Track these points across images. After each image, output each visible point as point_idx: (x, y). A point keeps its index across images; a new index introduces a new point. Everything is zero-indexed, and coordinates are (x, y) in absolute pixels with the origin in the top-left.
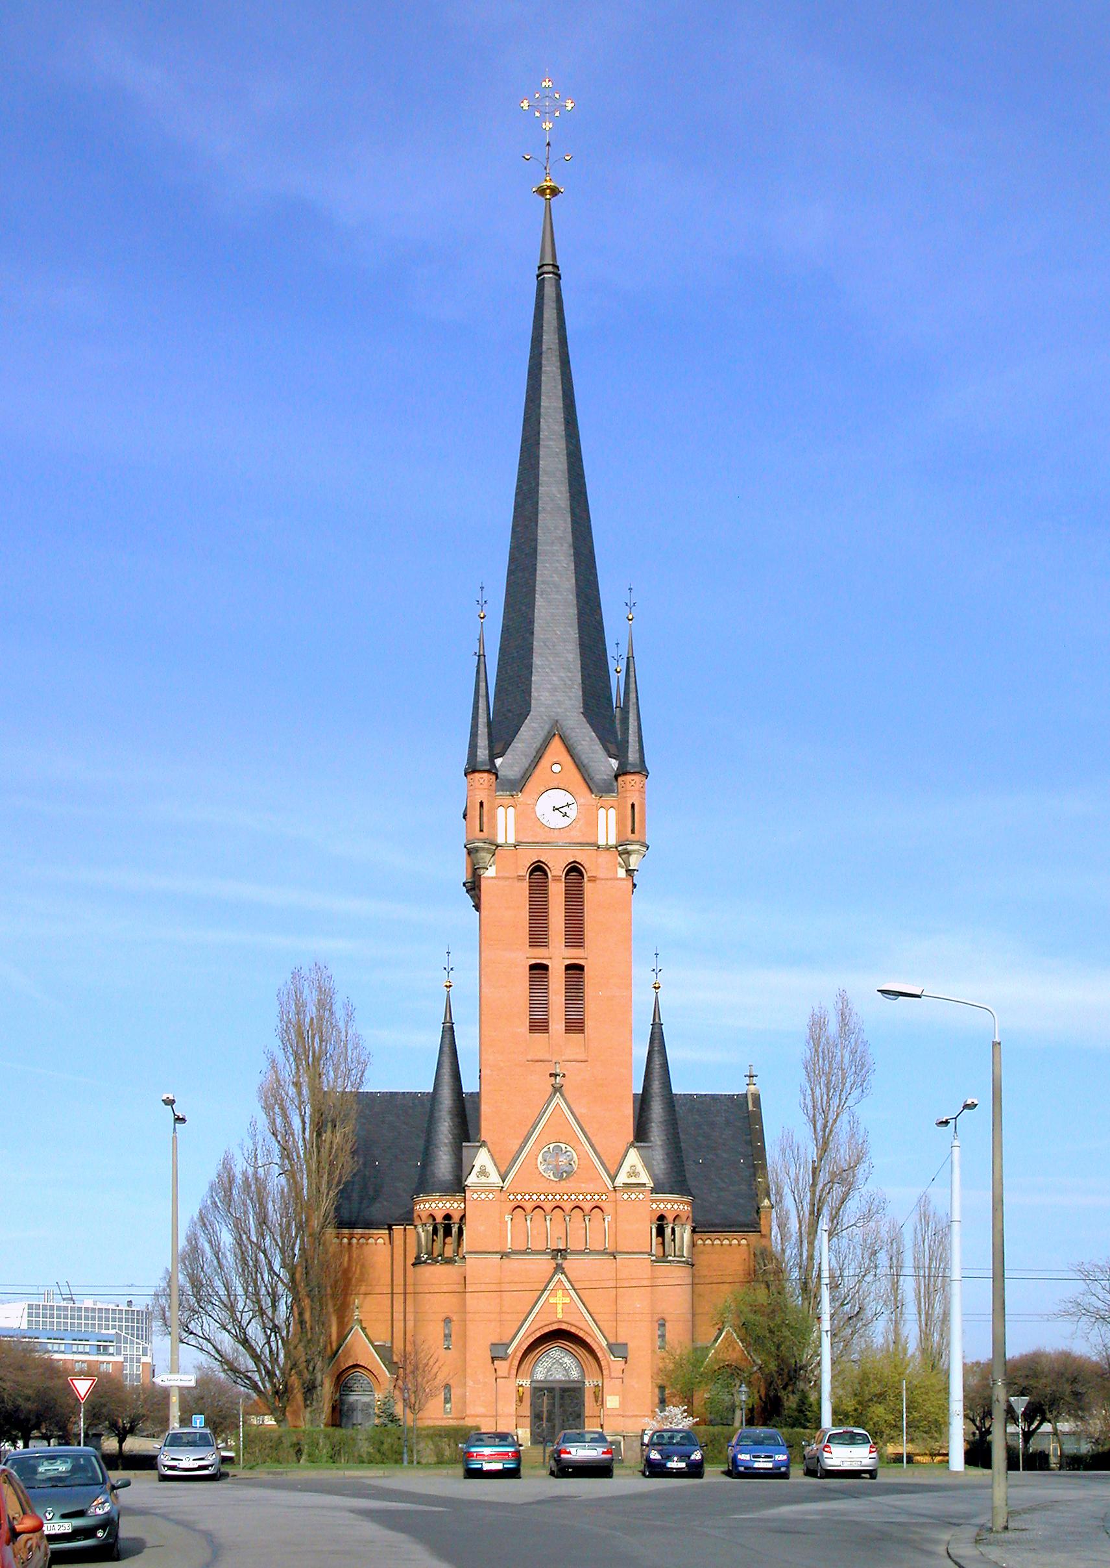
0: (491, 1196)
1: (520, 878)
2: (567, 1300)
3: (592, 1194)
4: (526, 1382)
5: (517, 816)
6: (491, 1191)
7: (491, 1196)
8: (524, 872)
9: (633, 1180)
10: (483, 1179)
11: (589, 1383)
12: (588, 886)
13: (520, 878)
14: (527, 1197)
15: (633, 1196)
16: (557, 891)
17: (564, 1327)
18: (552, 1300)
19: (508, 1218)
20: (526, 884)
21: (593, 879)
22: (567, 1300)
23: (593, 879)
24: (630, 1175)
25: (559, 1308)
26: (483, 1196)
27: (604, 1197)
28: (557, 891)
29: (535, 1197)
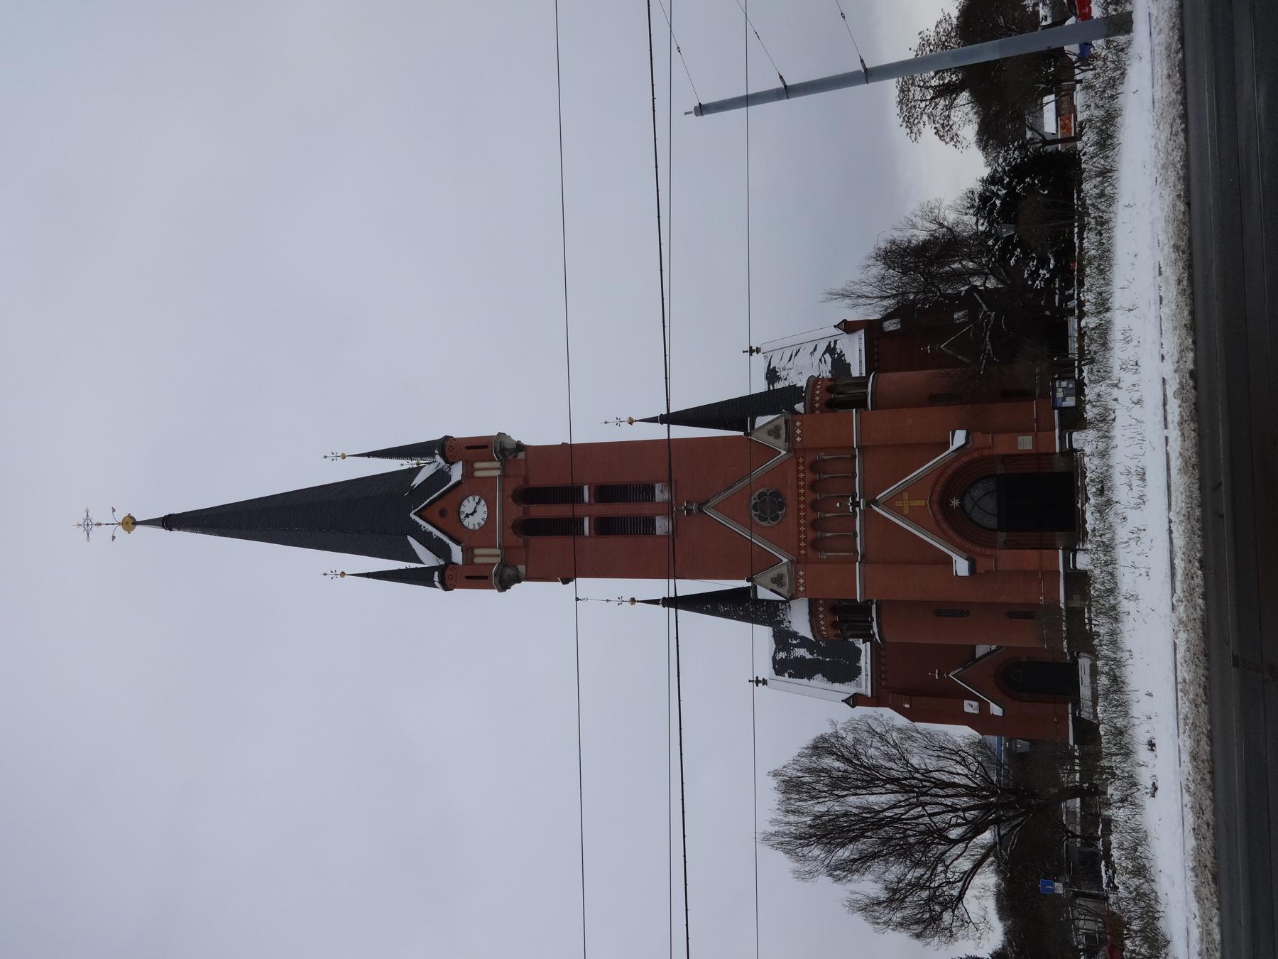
0: (801, 573)
1: (526, 545)
2: (906, 495)
3: (798, 472)
4: (1002, 537)
5: (480, 547)
6: (797, 571)
7: (801, 573)
8: (520, 542)
9: (783, 432)
10: (787, 580)
11: (1000, 470)
12: (534, 483)
13: (526, 545)
14: (803, 536)
15: (798, 431)
16: (539, 511)
17: (935, 498)
18: (906, 512)
19: (824, 556)
20: (532, 540)
21: (526, 479)
22: (906, 495)
23: (526, 479)
24: (778, 436)
25: (917, 503)
26: (801, 581)
27: (801, 460)
28: (539, 511)
29: (803, 529)
